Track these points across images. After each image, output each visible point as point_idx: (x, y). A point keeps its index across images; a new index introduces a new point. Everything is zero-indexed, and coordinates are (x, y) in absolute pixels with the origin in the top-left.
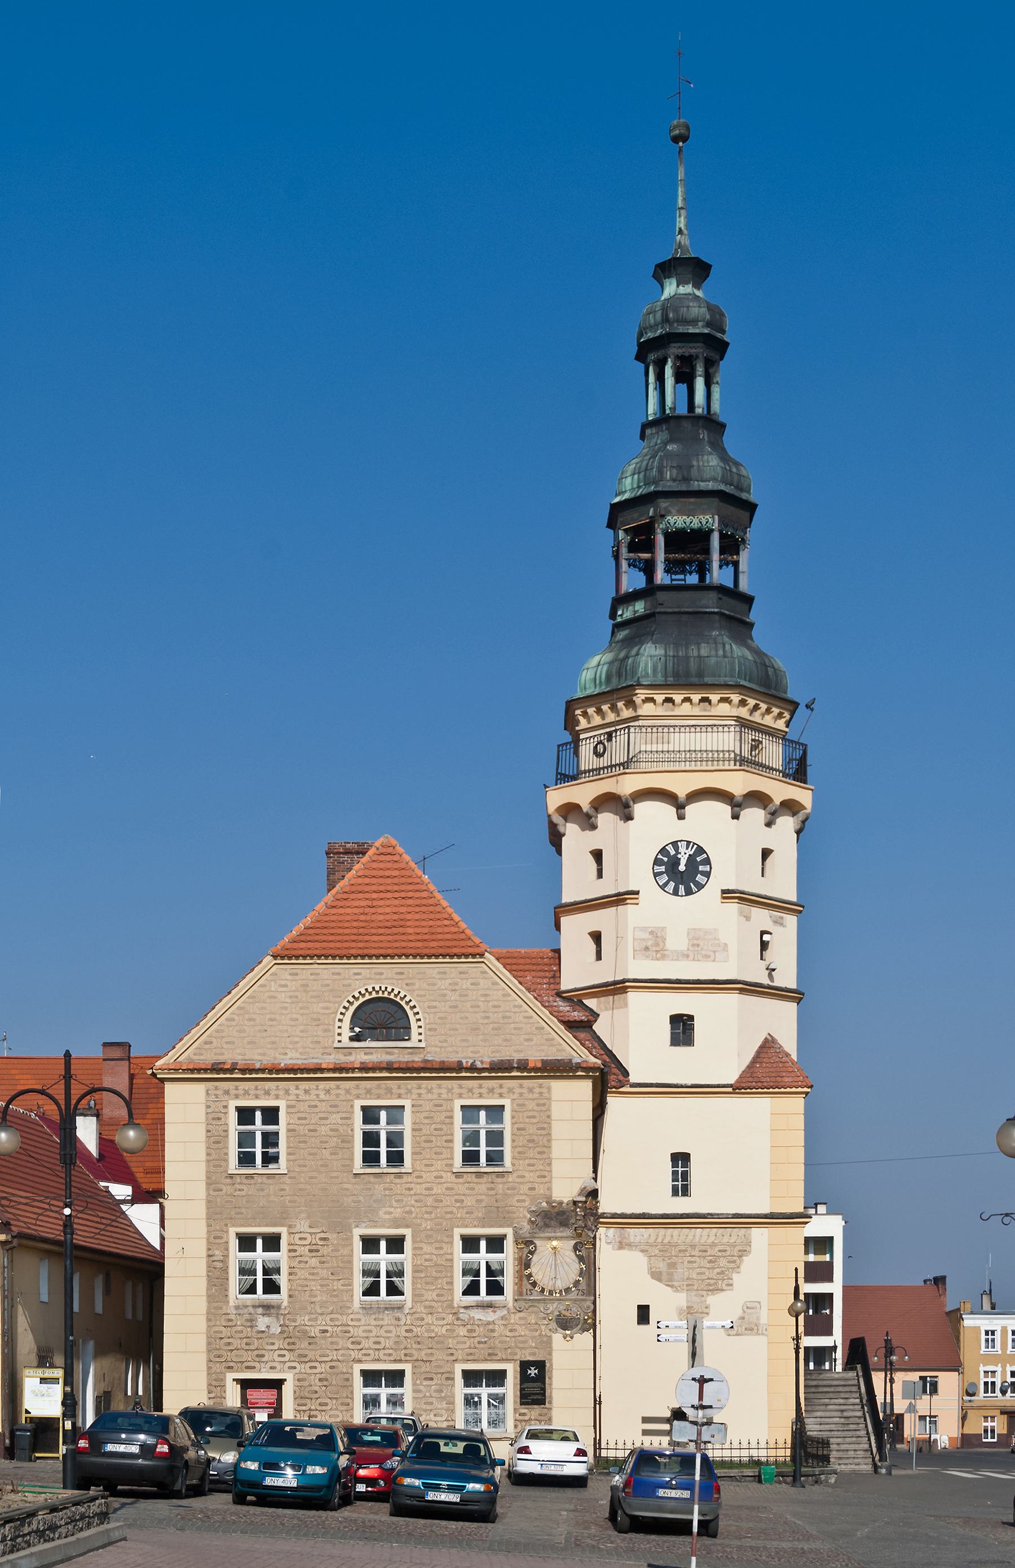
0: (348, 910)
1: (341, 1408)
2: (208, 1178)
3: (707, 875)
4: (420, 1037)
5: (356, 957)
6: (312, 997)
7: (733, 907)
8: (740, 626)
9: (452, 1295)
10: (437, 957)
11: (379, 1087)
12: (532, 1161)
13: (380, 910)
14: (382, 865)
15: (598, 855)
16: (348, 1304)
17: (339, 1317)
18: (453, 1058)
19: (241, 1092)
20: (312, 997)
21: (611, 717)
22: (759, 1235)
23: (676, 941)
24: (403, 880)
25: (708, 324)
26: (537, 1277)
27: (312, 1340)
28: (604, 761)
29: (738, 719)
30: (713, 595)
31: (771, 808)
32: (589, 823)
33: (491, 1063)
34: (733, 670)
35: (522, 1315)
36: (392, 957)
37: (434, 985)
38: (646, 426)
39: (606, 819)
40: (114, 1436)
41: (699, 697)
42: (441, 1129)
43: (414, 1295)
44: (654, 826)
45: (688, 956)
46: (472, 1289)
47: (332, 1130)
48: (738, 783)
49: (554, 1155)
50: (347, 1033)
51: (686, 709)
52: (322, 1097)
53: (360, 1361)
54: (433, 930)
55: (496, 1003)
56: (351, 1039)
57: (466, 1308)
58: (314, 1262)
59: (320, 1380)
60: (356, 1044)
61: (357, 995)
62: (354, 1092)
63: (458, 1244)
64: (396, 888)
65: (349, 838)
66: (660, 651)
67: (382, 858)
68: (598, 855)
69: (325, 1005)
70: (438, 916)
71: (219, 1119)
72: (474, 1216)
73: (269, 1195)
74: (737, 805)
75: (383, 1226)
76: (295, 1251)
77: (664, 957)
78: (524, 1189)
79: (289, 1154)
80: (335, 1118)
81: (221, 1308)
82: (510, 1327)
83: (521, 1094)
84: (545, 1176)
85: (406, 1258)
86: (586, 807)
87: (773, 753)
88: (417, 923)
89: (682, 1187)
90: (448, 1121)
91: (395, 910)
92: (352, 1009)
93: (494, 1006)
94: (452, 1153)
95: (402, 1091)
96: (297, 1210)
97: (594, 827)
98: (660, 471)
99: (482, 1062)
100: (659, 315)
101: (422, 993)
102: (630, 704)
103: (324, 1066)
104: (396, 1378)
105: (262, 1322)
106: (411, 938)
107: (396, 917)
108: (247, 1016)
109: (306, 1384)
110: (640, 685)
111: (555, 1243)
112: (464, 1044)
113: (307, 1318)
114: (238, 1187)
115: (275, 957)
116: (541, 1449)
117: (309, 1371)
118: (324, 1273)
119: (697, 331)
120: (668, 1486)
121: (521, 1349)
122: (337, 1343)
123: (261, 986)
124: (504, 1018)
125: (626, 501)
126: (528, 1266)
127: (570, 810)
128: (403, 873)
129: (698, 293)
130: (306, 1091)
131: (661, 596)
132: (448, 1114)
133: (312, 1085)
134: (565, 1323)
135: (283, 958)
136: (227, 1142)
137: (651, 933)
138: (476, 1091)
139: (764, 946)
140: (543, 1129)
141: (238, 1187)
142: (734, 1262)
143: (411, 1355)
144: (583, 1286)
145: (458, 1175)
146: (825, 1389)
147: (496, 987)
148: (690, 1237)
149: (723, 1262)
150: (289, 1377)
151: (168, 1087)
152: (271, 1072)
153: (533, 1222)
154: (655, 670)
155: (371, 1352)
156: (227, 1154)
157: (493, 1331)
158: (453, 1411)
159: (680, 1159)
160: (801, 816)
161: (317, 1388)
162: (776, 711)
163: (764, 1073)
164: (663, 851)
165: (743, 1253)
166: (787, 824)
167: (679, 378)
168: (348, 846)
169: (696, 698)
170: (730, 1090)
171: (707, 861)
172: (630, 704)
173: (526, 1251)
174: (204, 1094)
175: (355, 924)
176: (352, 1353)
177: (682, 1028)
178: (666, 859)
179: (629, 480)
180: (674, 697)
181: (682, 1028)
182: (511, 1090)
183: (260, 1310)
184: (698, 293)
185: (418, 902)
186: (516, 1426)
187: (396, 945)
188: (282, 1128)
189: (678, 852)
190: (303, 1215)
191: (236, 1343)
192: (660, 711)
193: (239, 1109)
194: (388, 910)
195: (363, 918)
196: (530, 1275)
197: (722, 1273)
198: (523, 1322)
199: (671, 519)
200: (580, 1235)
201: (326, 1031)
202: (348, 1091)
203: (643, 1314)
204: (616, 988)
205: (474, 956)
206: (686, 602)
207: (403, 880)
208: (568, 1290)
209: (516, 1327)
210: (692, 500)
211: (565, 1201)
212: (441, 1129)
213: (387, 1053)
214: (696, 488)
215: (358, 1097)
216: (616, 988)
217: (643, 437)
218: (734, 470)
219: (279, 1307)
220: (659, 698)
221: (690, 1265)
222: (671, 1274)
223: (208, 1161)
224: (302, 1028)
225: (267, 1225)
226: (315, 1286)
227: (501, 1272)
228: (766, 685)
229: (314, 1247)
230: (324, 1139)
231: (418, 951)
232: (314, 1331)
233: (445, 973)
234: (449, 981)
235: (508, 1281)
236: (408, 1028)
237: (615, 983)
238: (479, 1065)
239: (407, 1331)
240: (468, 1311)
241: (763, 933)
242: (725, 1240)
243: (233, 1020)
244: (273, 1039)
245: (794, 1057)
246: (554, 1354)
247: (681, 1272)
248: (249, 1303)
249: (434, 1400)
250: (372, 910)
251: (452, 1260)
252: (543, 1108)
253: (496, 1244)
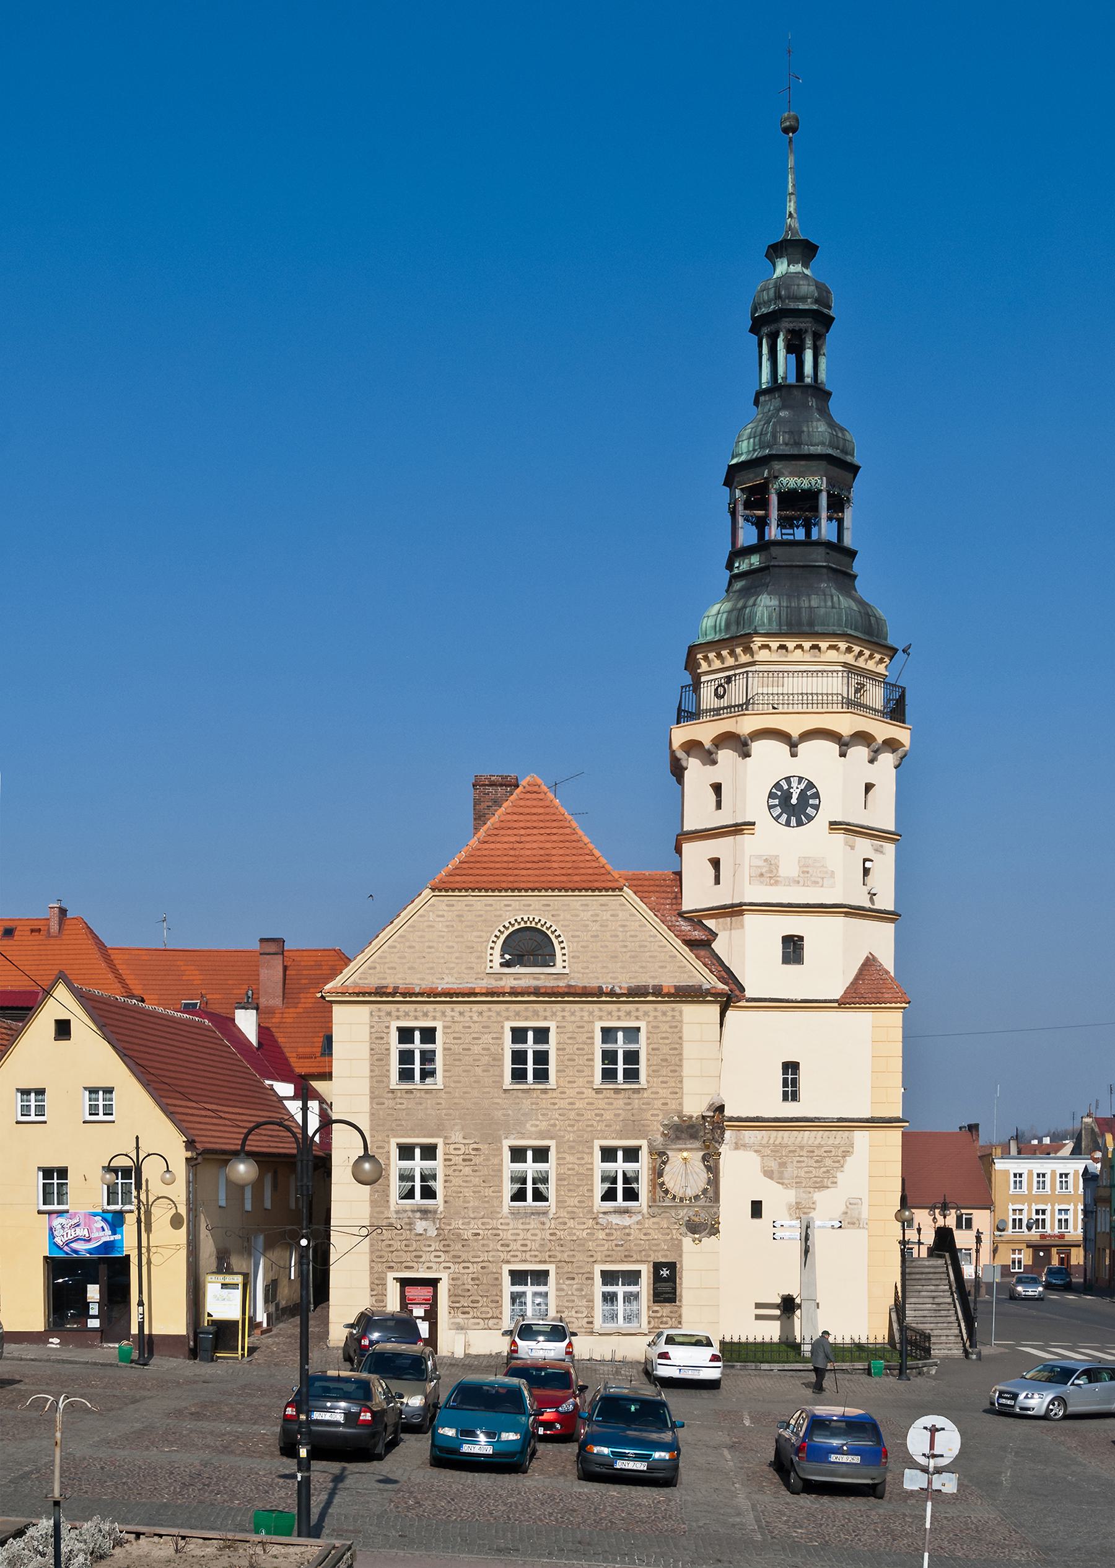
0: (498, 846)
1: (491, 1305)
2: (372, 1092)
3: (816, 808)
4: (565, 964)
5: (506, 891)
6: (467, 926)
7: (840, 837)
8: (845, 579)
9: (592, 1201)
10: (580, 890)
11: (526, 1009)
12: (665, 1079)
13: (528, 846)
14: (529, 803)
15: (717, 788)
16: (498, 1210)
17: (490, 1221)
18: (594, 984)
19: (401, 1014)
20: (467, 926)
21: (730, 661)
22: (861, 1138)
23: (788, 868)
24: (548, 817)
25: (816, 301)
26: (669, 1185)
27: (465, 1243)
28: (724, 702)
29: (845, 664)
30: (821, 550)
31: (874, 746)
32: (709, 758)
33: (629, 988)
34: (840, 619)
35: (655, 1220)
36: (540, 891)
37: (577, 916)
38: (760, 393)
39: (725, 756)
40: (320, 1403)
41: (810, 644)
42: (583, 1049)
43: (558, 1202)
44: (769, 762)
45: (798, 882)
46: (609, 1195)
47: (484, 1049)
48: (846, 724)
49: (684, 1074)
50: (497, 960)
51: (798, 655)
52: (475, 1018)
53: (508, 1262)
54: (575, 865)
55: (633, 933)
56: (502, 965)
57: (605, 1213)
58: (467, 1170)
59: (472, 1279)
60: (506, 970)
61: (507, 925)
62: (504, 1014)
63: (598, 1154)
64: (542, 824)
65: (495, 770)
66: (774, 602)
67: (529, 796)
68: (717, 788)
69: (479, 934)
70: (581, 851)
71: (382, 1038)
72: (612, 1128)
73: (426, 1109)
74: (844, 744)
75: (530, 1138)
76: (450, 1160)
77: (777, 883)
78: (658, 1104)
79: (445, 1071)
80: (487, 1038)
81: (383, 1213)
82: (644, 1231)
83: (655, 1017)
84: (677, 1092)
85: (550, 1167)
86: (708, 745)
87: (875, 696)
88: (562, 858)
89: (791, 1092)
90: (589, 1041)
91: (542, 845)
92: (503, 937)
93: (631, 936)
94: (593, 1071)
95: (548, 1014)
96: (452, 1122)
97: (714, 762)
98: (774, 436)
99: (620, 988)
100: (772, 292)
101: (566, 923)
102: (748, 650)
103: (477, 991)
104: (540, 1277)
105: (420, 1226)
106: (556, 872)
107: (542, 852)
108: (407, 944)
109: (459, 1282)
110: (757, 633)
111: (685, 1154)
112: (604, 970)
113: (460, 1222)
114: (399, 1101)
115: (433, 890)
116: (679, 1355)
117: (463, 1271)
118: (476, 1181)
119: (807, 307)
120: (838, 1451)
121: (655, 1251)
122: (487, 1245)
123: (421, 916)
124: (640, 946)
125: (742, 462)
126: (661, 1175)
127: (693, 747)
128: (548, 810)
129: (806, 272)
130: (461, 1014)
131: (775, 551)
132: (589, 1035)
133: (467, 1007)
134: (693, 1228)
135: (440, 891)
136: (389, 1060)
137: (766, 860)
138: (615, 1014)
139: (866, 872)
140: (676, 1049)
141: (399, 1101)
142: (839, 1162)
143: (555, 1256)
144: (711, 1194)
145: (598, 1091)
146: (918, 1276)
147: (634, 918)
148: (799, 1139)
150: (444, 1276)
151: (335, 1007)
152: (429, 996)
153: (665, 1135)
154: (770, 619)
155: (519, 1254)
156: (388, 1071)
157: (629, 1235)
158: (592, 1308)
159: (791, 1068)
160: (900, 752)
161: (469, 1287)
162: (878, 656)
163: (866, 990)
164: (777, 785)
165: (846, 1153)
166: (887, 759)
167: (790, 349)
168: (493, 778)
169: (807, 645)
170: (836, 1005)
171: (817, 795)
172: (748, 650)
173: (659, 1161)
174: (368, 1015)
175: (505, 859)
176: (501, 1254)
177: (793, 949)
178: (779, 793)
179: (745, 444)
180: (788, 644)
181: (793, 949)
182: (646, 1014)
183: (418, 1215)
184: (806, 272)
185: (562, 838)
186: (649, 1323)
187: (543, 879)
188: (438, 1047)
189: (790, 787)
190: (457, 1128)
191: (397, 1245)
192: (775, 657)
193: (400, 1029)
194: (535, 845)
195: (512, 852)
196: (663, 1183)
197: (828, 1171)
198: (656, 1226)
199: (784, 480)
200: (708, 1147)
201: (478, 958)
202: (498, 1014)
203: (757, 1209)
204: (734, 911)
205: (614, 890)
206: (798, 556)
207: (548, 817)
208: (697, 1197)
209: (650, 1231)
210: (803, 463)
211: (695, 1115)
212: (583, 1049)
213: (534, 978)
214: (806, 452)
215: (508, 1019)
216: (734, 911)
217: (756, 403)
218: (840, 435)
219: (435, 1212)
220: (774, 645)
221: (799, 1165)
222: (781, 1173)
223: (372, 1077)
224: (457, 955)
225: (424, 1137)
226: (468, 1193)
227: (636, 1180)
228: (869, 633)
229: (467, 1157)
230: (477, 1057)
231: (563, 885)
232: (467, 1235)
233: (587, 905)
234: (590, 913)
235: (643, 1188)
236: (553, 955)
237: (732, 906)
238: (618, 991)
239: (551, 1234)
240: (606, 1217)
241: (865, 860)
242: (830, 1142)
243: (395, 947)
244: (431, 965)
245: (892, 974)
246: (684, 1256)
247: (791, 1171)
248: (408, 1208)
249: (575, 1298)
250: (521, 846)
251: (592, 1169)
252: (676, 1030)
253: (632, 1154)
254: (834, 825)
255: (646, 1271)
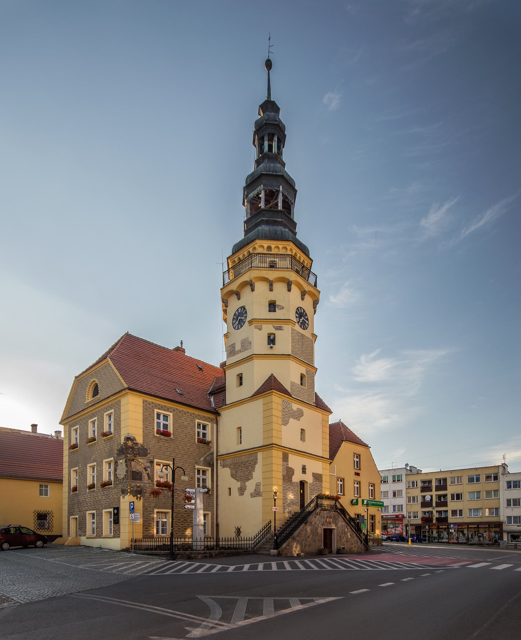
149: (250, 468)
165: (256, 463)
197: (250, 472)
254: (251, 322)
255: (112, 510)
